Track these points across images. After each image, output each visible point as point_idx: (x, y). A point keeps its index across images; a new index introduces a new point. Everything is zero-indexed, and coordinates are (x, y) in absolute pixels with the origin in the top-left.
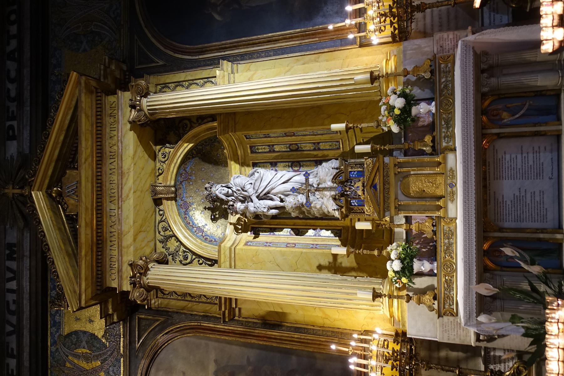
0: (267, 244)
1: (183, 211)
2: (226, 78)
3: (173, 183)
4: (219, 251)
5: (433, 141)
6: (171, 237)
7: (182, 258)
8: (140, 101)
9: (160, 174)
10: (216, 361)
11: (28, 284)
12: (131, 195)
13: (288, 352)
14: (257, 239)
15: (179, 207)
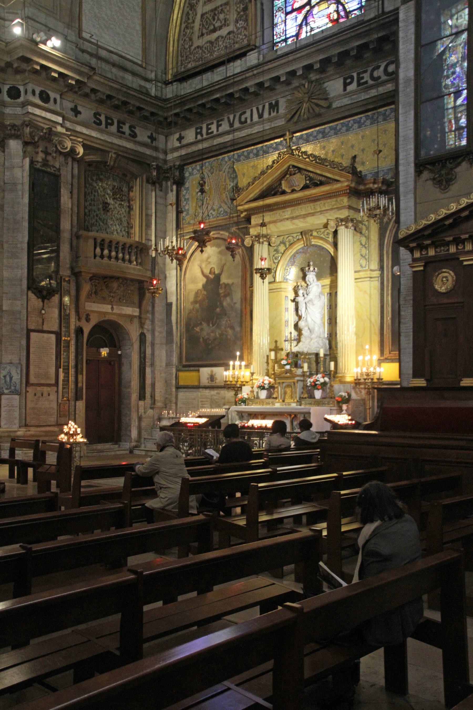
0: (287, 310)
1: (301, 250)
2: (366, 276)
3: (313, 243)
4: (279, 282)
5: (305, 398)
6: (285, 246)
7: (276, 255)
8: (342, 225)
9: (318, 232)
10: (233, 284)
11: (256, 131)
12: (294, 226)
13: (241, 326)
14: (290, 302)
15: (303, 248)
